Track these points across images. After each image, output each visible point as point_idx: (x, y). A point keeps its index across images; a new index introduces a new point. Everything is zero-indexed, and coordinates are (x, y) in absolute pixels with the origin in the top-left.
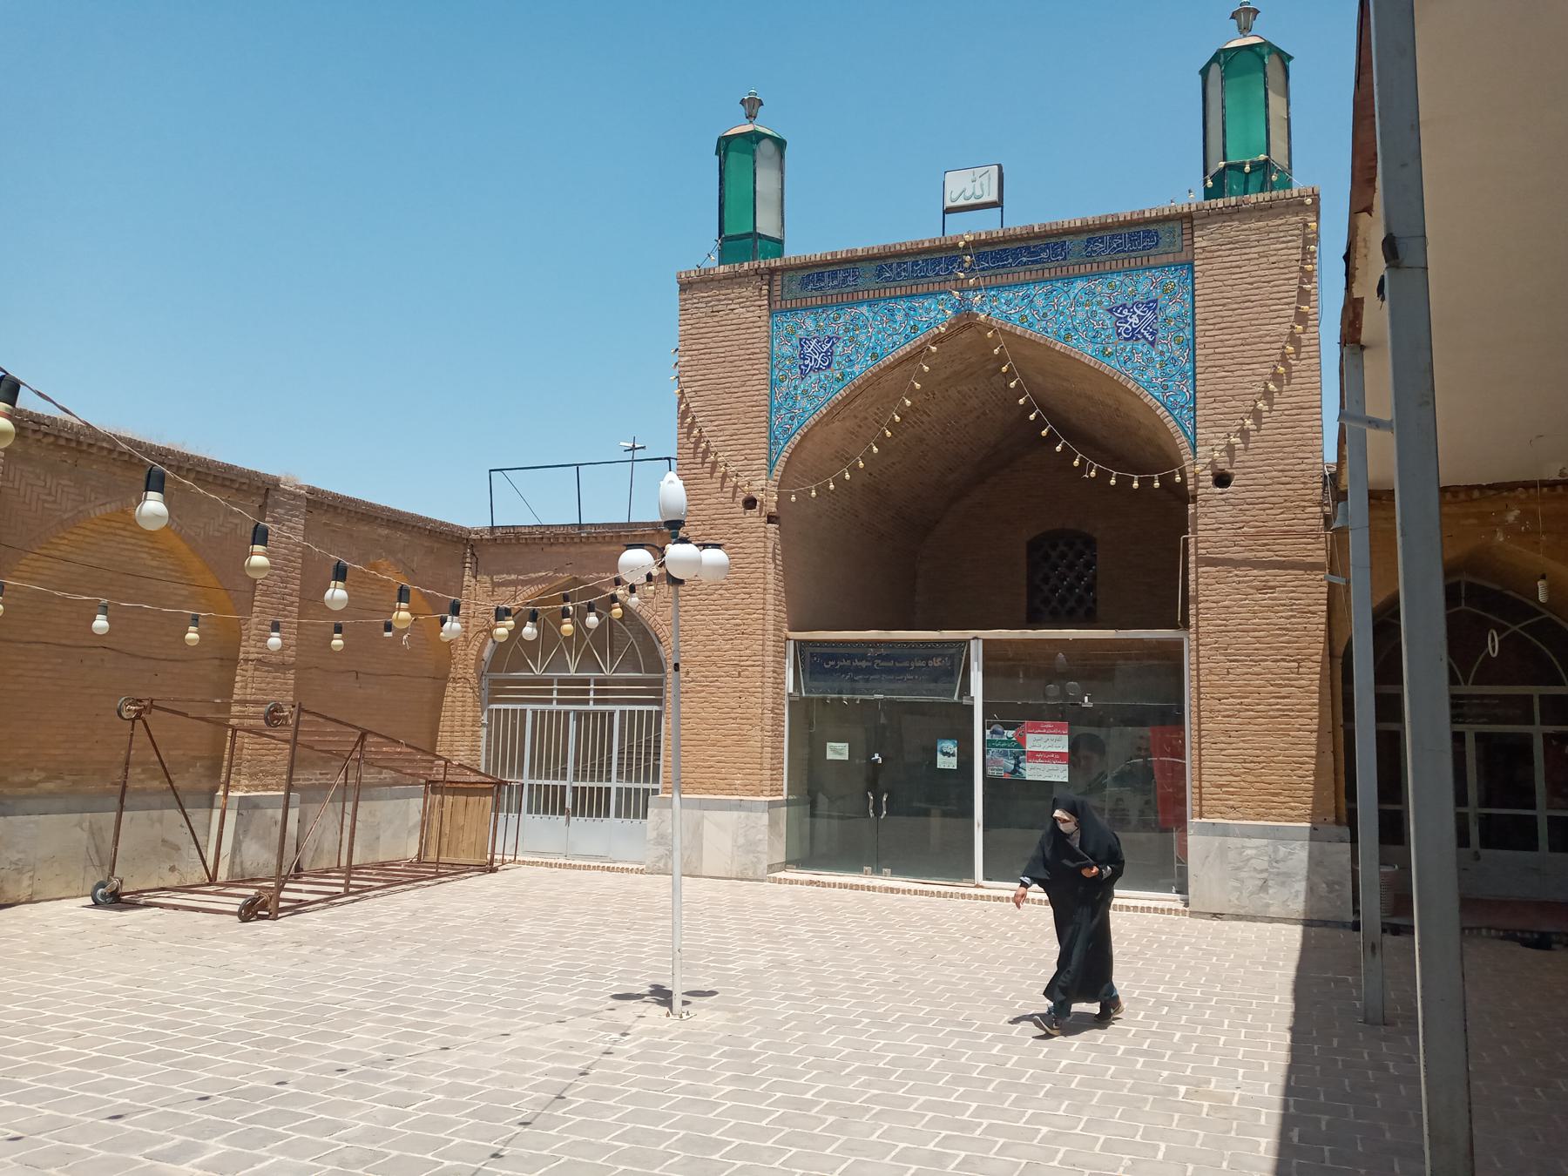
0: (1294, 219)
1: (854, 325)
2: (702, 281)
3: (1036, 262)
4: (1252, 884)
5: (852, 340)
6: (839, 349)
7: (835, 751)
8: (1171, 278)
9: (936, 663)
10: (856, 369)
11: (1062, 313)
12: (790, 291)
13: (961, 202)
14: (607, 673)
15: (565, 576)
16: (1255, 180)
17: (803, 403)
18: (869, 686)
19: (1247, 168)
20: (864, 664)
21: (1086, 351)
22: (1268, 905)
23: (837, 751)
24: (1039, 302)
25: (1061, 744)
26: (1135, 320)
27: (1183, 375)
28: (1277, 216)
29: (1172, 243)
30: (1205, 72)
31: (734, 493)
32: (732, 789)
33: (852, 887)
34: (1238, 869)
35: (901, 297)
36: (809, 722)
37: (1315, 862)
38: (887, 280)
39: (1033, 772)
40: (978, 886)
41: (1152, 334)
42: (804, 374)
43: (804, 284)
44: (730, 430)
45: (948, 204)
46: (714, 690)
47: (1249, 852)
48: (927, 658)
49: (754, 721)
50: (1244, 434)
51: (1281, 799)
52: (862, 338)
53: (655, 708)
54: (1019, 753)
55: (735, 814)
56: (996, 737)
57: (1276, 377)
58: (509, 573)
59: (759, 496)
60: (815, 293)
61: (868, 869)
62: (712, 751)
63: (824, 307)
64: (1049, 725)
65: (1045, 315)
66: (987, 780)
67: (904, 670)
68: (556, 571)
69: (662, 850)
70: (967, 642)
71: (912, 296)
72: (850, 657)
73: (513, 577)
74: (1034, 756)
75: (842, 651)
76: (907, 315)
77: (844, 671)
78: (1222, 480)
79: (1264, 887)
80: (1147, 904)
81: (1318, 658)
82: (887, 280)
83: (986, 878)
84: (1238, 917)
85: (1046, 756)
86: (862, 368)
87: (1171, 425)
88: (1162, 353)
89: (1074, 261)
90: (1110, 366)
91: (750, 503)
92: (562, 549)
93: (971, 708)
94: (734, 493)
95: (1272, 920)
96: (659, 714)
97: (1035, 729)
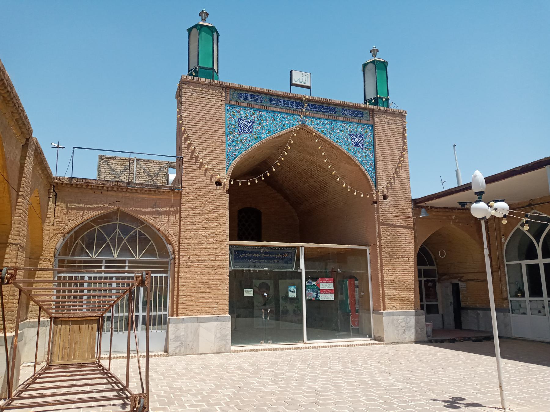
0: (400, 119)
1: (261, 118)
2: (194, 82)
3: (326, 112)
4: (401, 332)
5: (260, 124)
6: (255, 126)
7: (247, 293)
8: (367, 129)
9: (285, 255)
10: (263, 136)
11: (335, 132)
12: (233, 98)
13: (298, 83)
14: (137, 258)
15: (114, 208)
16: (385, 104)
17: (240, 145)
18: (262, 264)
19: (384, 100)
20: (257, 255)
21: (343, 148)
22: (405, 338)
23: (248, 292)
24: (328, 126)
25: (330, 286)
26: (357, 140)
27: (371, 161)
28: (396, 117)
29: (367, 117)
30: (365, 66)
31: (211, 178)
32: (214, 312)
33: (269, 350)
34: (397, 327)
35: (279, 112)
36: (237, 281)
37: (417, 322)
38: (274, 104)
39: (323, 297)
40: (305, 343)
41: (362, 146)
42: (240, 133)
43: (240, 96)
44: (209, 150)
45: (293, 82)
46: (202, 266)
47: (400, 321)
48: (282, 254)
49: (223, 280)
50: (391, 183)
51: (406, 302)
52: (264, 124)
53: (164, 275)
54: (318, 291)
55: (215, 323)
56: (309, 284)
57: (398, 167)
58: (78, 203)
59: (223, 181)
60: (245, 102)
61: (262, 341)
62: (203, 295)
63: (249, 108)
64: (327, 279)
65: (330, 132)
66: (307, 301)
67: (273, 258)
68: (110, 204)
69: (177, 344)
70: (299, 247)
71: (283, 113)
72: (252, 252)
73: (81, 205)
74: (323, 291)
75: (248, 250)
76: (281, 119)
77: (249, 258)
78: (385, 197)
79: (404, 332)
80: (357, 343)
81: (413, 257)
82: (274, 104)
83: (308, 340)
84: (398, 343)
85: (326, 291)
86: (265, 136)
87: (369, 177)
88: (365, 153)
89: (338, 115)
90: (351, 154)
91: (218, 184)
92: (114, 194)
93: (301, 273)
94: (211, 178)
95: (407, 343)
96: (166, 278)
97: (322, 281)
